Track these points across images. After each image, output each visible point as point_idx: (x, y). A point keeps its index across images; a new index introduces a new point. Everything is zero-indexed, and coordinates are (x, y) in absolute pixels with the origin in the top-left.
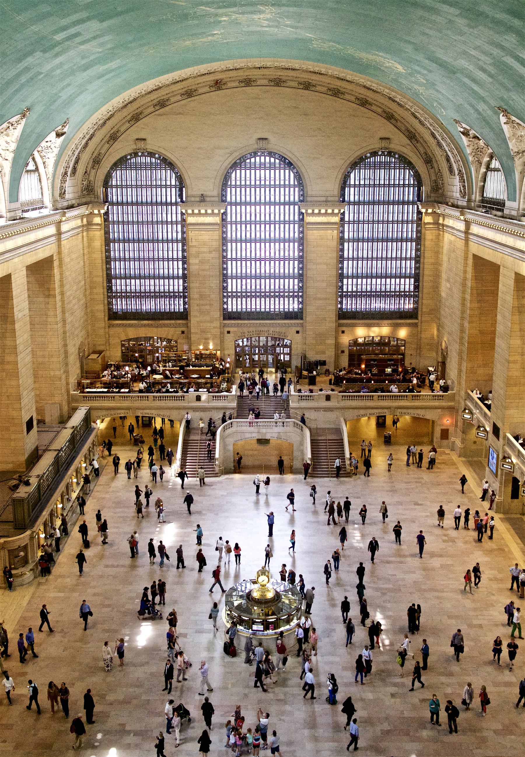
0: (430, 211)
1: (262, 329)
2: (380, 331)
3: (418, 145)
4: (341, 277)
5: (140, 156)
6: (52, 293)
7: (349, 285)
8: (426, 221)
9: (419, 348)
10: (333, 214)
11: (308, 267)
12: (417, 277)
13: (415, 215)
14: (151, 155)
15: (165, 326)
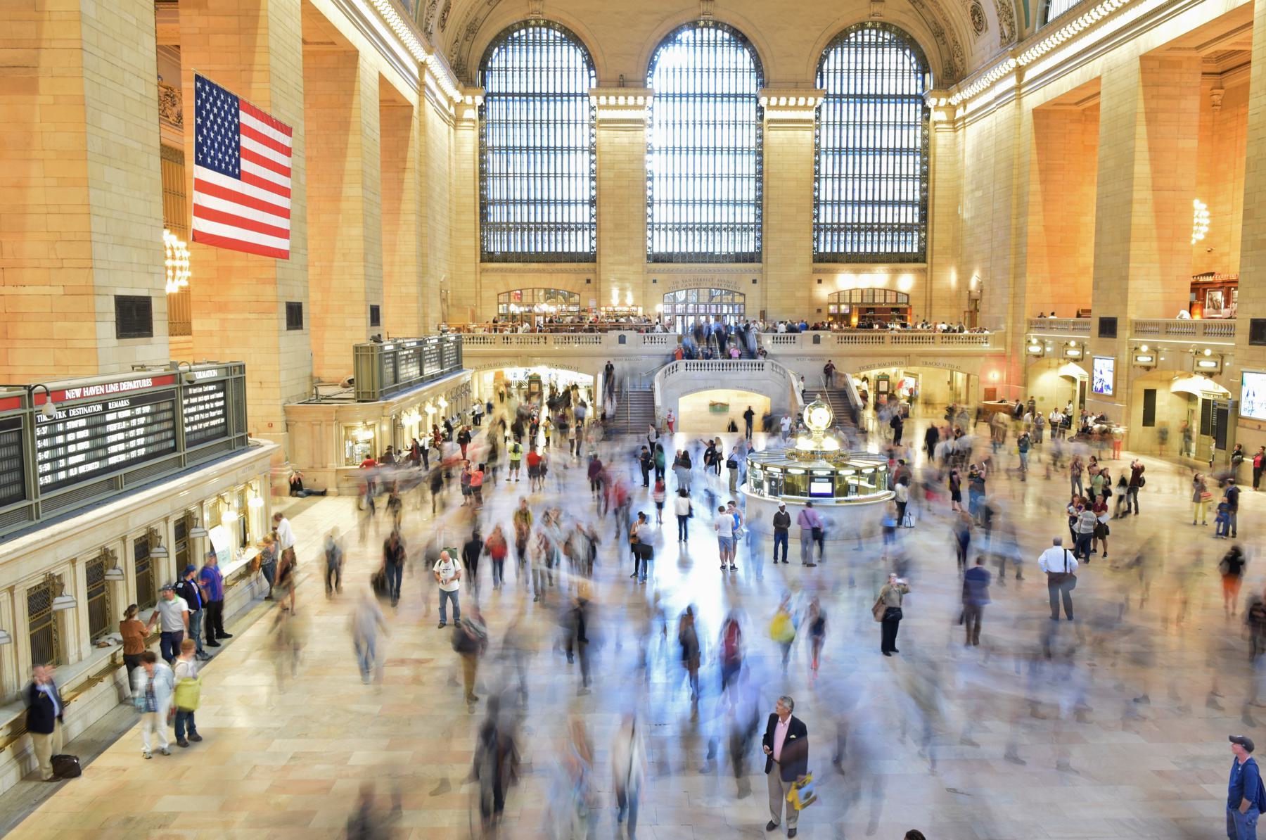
0: (943, 102)
1: (703, 276)
2: (876, 279)
3: (924, 11)
4: (817, 203)
5: (534, 27)
6: (409, 165)
7: (826, 215)
8: (937, 119)
9: (929, 305)
10: (806, 107)
11: (770, 184)
12: (924, 206)
13: (919, 114)
14: (549, 25)
15: (562, 271)
